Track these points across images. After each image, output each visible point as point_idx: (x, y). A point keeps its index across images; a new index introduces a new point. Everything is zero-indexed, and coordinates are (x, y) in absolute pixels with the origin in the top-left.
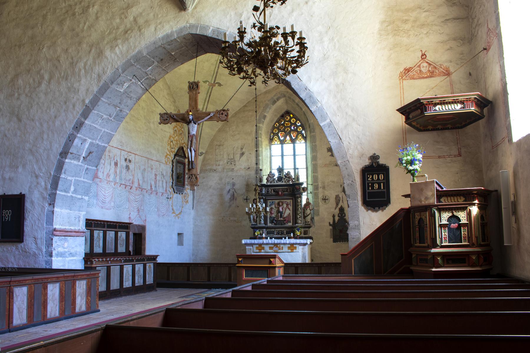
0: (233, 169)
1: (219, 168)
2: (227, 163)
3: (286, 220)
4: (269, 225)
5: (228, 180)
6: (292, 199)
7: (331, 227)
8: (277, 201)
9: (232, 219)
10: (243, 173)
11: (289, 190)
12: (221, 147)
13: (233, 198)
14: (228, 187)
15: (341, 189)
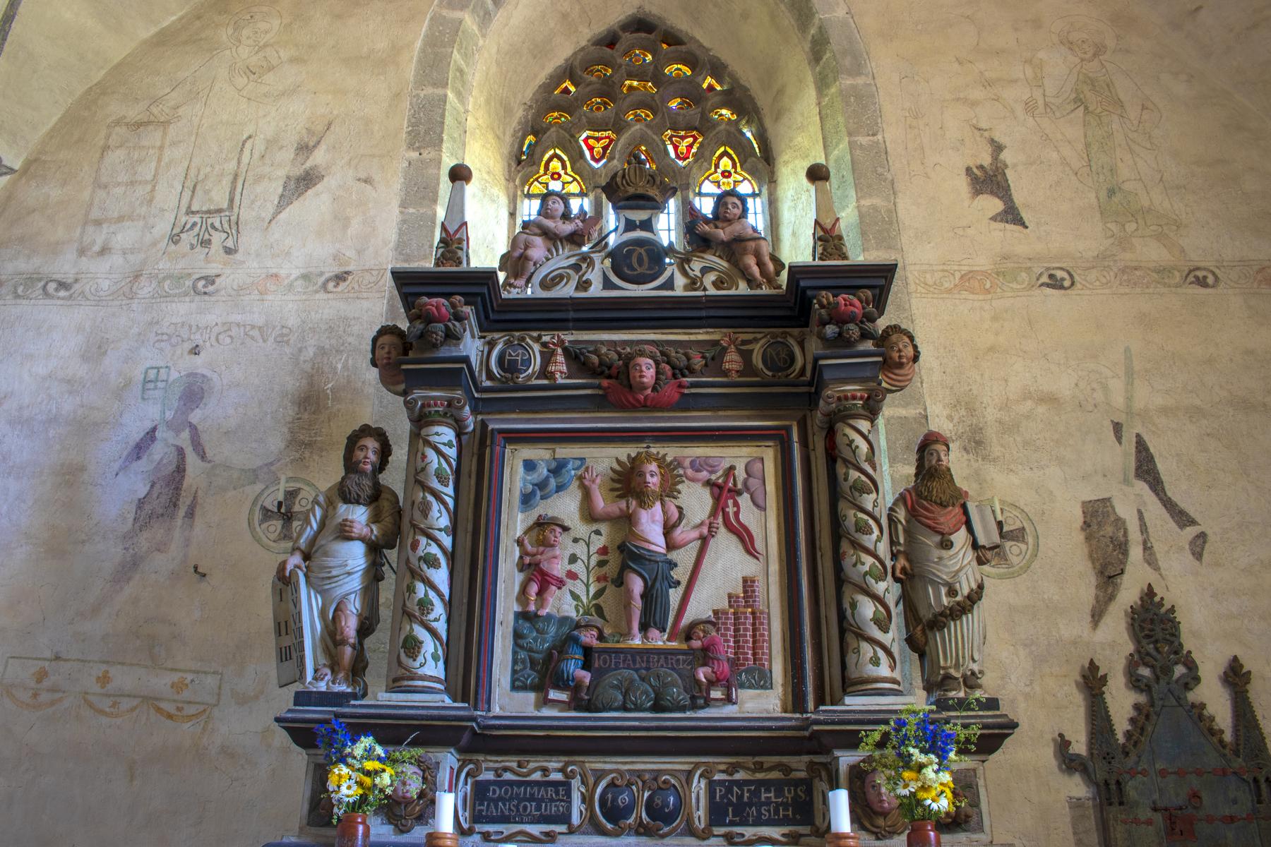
0: (210, 280)
1: (103, 274)
2: (175, 239)
3: (706, 657)
4: (508, 701)
5: (149, 357)
6: (781, 439)
7: (1077, 787)
8: (604, 459)
9: (124, 679)
10: (286, 307)
11: (732, 360)
12: (152, 137)
13: (171, 496)
14: (144, 414)
15: (1121, 457)
